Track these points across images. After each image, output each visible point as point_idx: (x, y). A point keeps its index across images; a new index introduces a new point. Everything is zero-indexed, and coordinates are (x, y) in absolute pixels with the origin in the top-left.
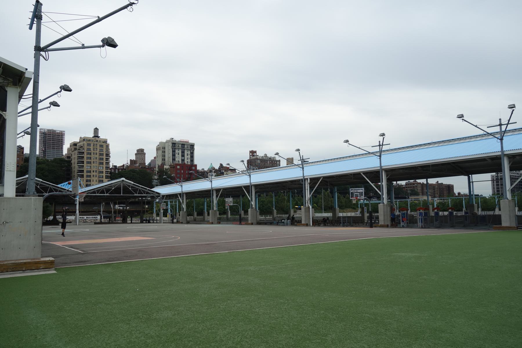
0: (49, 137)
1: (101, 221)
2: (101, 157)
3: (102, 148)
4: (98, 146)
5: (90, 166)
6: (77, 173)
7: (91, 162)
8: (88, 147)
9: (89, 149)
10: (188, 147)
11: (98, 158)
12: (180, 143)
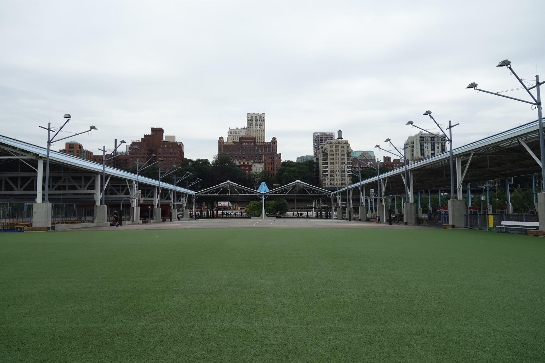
0: (321, 140)
1: (307, 217)
2: (342, 157)
3: (344, 149)
4: (340, 147)
5: (333, 167)
6: (323, 173)
7: (334, 163)
8: (331, 149)
9: (332, 151)
10: (439, 139)
11: (340, 159)
12: (429, 136)
